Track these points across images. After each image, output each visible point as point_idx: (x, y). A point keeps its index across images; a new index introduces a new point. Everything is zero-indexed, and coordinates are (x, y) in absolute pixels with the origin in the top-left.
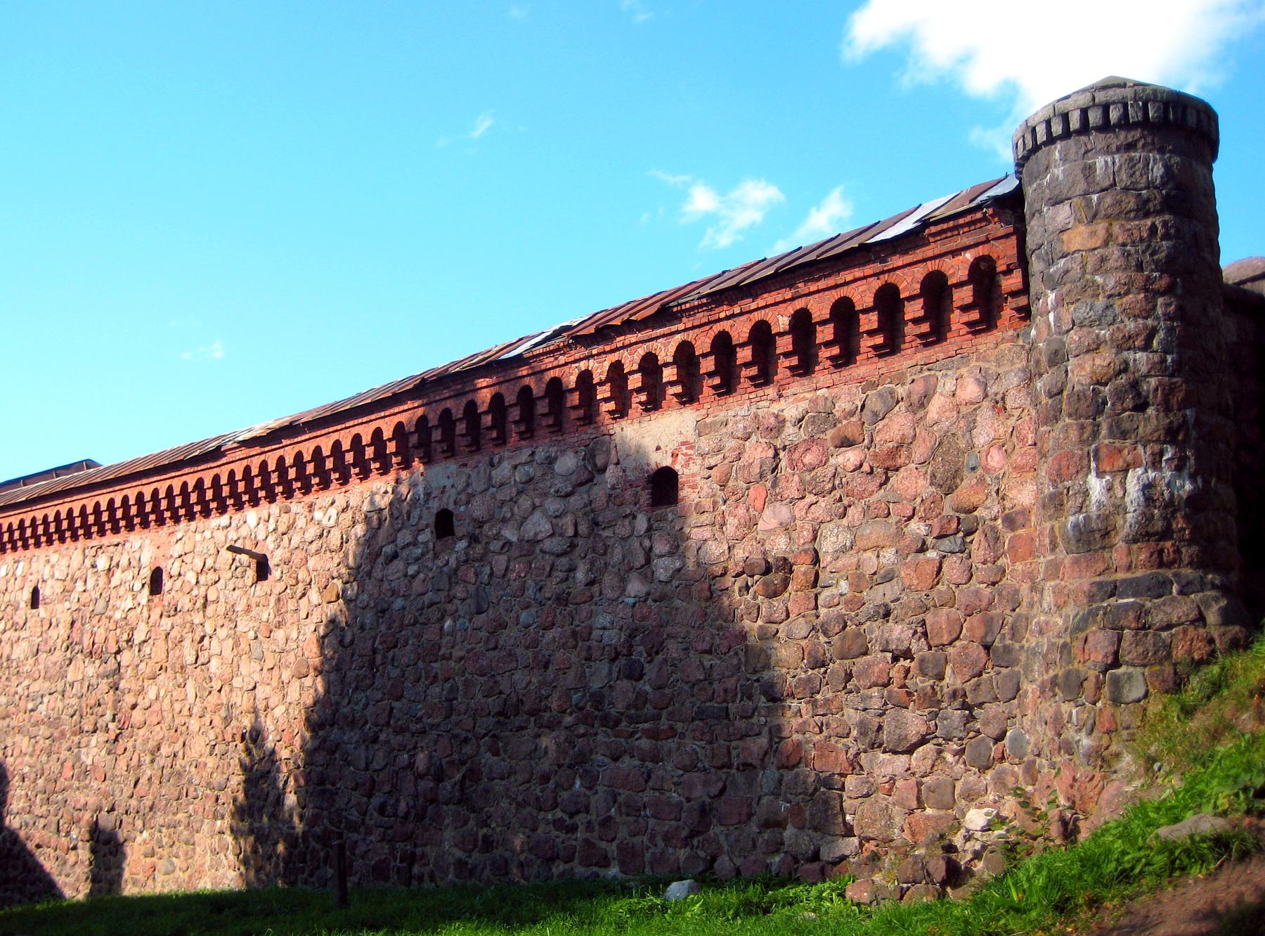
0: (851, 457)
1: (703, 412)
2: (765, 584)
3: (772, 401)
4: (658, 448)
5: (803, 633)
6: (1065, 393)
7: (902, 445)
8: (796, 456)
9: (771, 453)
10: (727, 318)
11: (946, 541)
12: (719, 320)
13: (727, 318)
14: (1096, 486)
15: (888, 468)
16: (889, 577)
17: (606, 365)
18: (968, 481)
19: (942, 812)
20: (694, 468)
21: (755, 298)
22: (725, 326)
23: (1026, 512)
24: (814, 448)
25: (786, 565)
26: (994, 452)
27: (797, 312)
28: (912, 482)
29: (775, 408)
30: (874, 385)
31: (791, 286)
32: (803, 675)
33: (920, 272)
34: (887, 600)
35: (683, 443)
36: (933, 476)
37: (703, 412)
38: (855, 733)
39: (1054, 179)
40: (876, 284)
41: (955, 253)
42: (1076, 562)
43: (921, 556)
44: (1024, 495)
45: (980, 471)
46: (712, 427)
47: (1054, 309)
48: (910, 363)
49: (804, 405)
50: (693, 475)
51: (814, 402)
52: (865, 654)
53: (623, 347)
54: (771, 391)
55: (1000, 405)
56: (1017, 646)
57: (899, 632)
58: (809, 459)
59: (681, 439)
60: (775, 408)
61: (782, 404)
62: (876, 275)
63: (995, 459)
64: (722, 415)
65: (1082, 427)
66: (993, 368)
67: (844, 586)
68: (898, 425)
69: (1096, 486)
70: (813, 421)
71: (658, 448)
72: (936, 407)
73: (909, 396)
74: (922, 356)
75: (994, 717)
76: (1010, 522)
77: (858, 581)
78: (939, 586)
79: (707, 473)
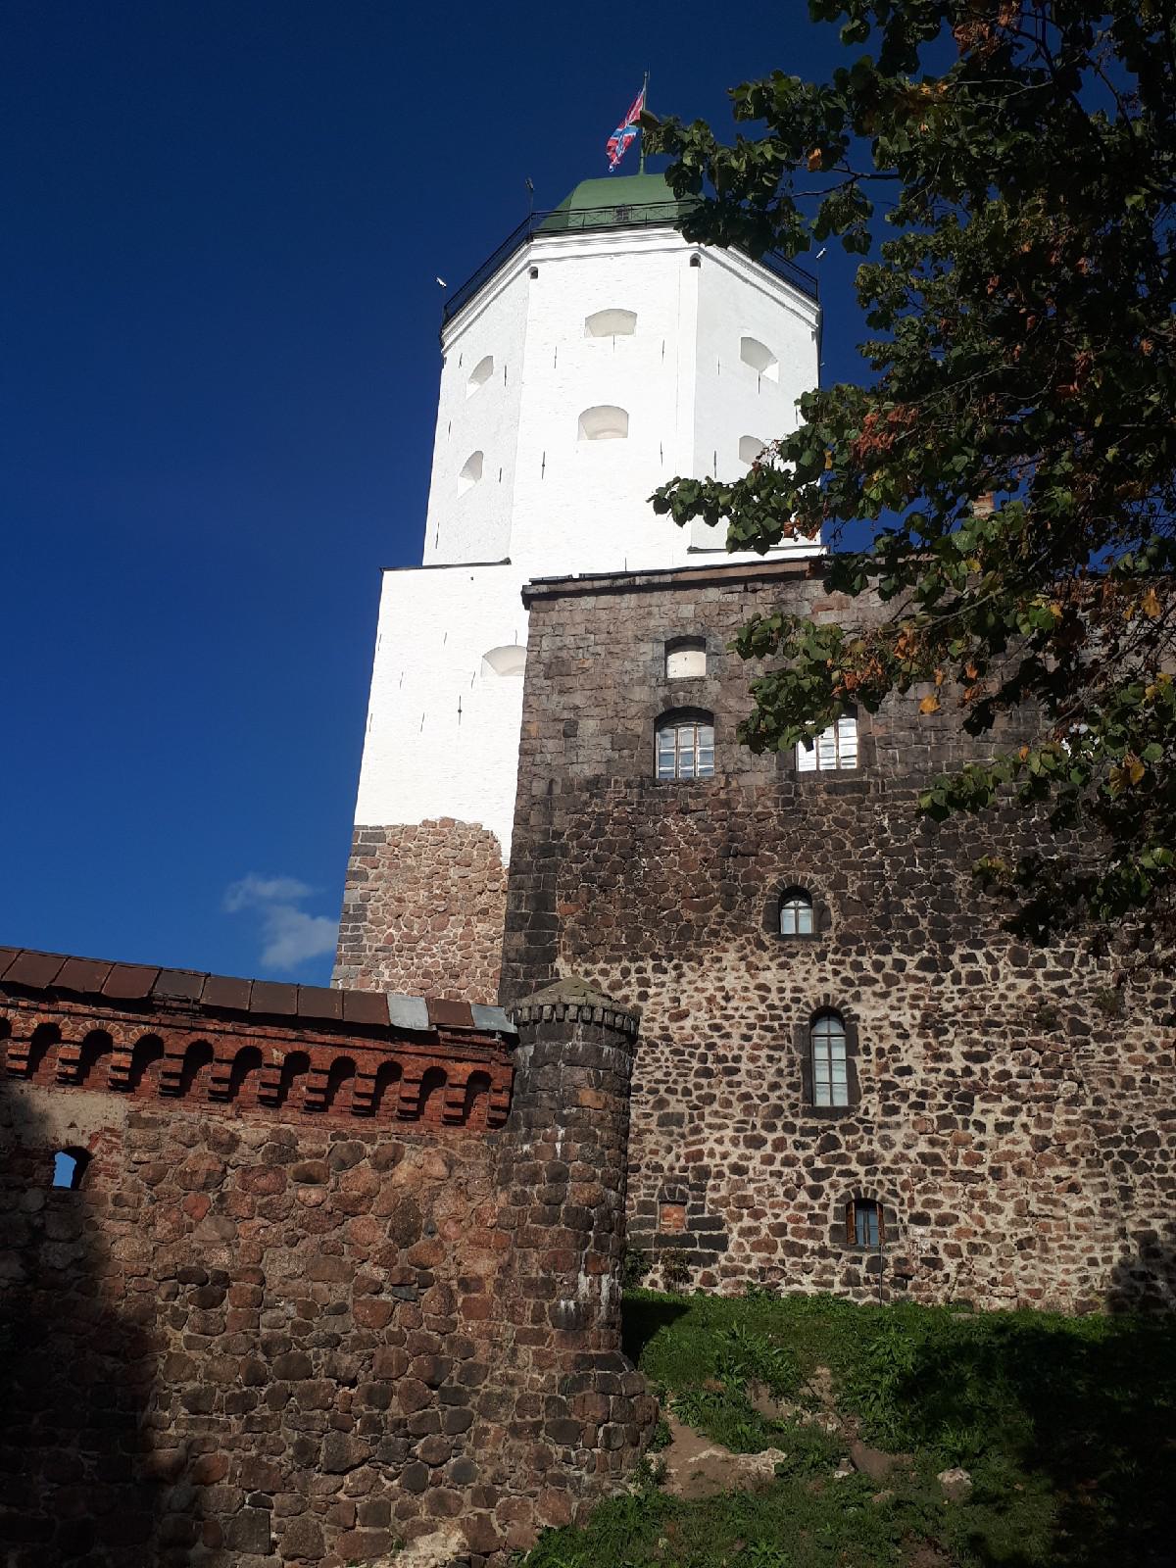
0: (314, 1194)
1: (139, 1104)
2: (201, 1294)
3: (229, 1118)
4: (73, 1125)
5: (242, 1349)
6: (563, 1207)
7: (369, 1195)
8: (249, 1178)
9: (220, 1168)
10: (214, 1031)
11: (403, 1289)
12: (204, 1030)
13: (214, 1031)
14: (584, 1281)
15: (351, 1208)
16: (341, 1310)
17: (34, 1023)
18: (424, 1240)
19: (378, 1530)
20: (116, 1158)
21: (252, 1024)
22: (210, 1038)
23: (479, 1279)
24: (271, 1175)
25: (223, 1279)
26: (450, 1223)
27: (296, 1053)
28: (372, 1231)
29: (230, 1126)
30: (344, 1137)
31: (295, 1029)
32: (237, 1391)
33: (425, 1063)
34: (337, 1331)
35: (107, 1129)
36: (393, 1230)
37: (139, 1104)
38: (290, 1451)
39: (574, 1048)
40: (384, 1058)
41: (459, 1060)
42: (562, 1336)
43: (375, 1298)
44: (483, 1266)
45: (437, 1237)
46: (150, 1123)
47: (562, 1141)
48: (383, 1128)
49: (264, 1133)
50: (115, 1164)
51: (276, 1133)
52: (310, 1376)
53: (69, 1013)
54: (229, 1109)
55: (461, 1189)
56: (468, 1389)
57: (347, 1361)
58: (263, 1182)
59: (108, 1124)
60: (230, 1126)
61: (239, 1124)
62: (384, 1051)
63: (451, 1229)
64: (162, 1113)
65: (578, 1236)
66: (457, 1154)
67: (292, 1310)
68: (364, 1175)
69: (584, 1281)
70: (273, 1150)
71: (73, 1125)
72: (402, 1173)
73: (375, 1155)
74: (394, 1127)
75: (438, 1446)
76: (465, 1284)
77: (308, 1310)
78: (390, 1327)
79: (133, 1167)
